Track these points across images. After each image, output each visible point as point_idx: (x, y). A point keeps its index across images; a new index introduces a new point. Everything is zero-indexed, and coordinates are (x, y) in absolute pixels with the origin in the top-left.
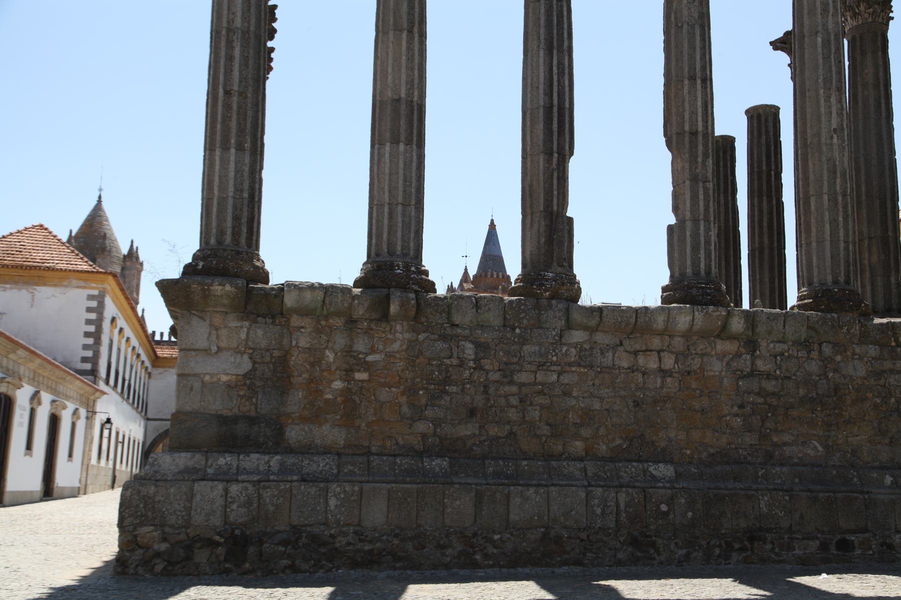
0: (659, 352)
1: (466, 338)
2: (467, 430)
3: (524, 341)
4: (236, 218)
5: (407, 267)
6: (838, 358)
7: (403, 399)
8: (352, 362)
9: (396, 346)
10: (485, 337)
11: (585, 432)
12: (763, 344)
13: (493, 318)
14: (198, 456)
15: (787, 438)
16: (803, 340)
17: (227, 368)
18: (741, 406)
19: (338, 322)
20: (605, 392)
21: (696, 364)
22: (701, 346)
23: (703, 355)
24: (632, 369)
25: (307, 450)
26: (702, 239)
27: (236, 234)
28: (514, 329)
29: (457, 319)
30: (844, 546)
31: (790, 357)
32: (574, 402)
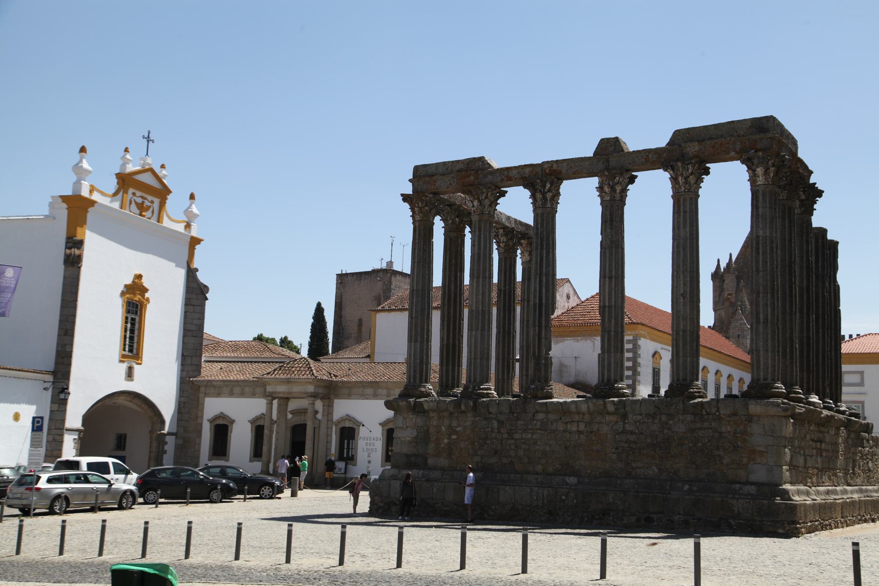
2: (493, 460)
3: (518, 419)
4: (415, 371)
5: (474, 387)
6: (671, 422)
7: (470, 447)
8: (452, 431)
9: (468, 423)
10: (501, 418)
12: (630, 416)
14: (397, 470)
17: (405, 435)
18: (617, 449)
19: (446, 414)
21: (595, 427)
23: (598, 423)
24: (565, 431)
25: (434, 468)
26: (606, 363)
27: (415, 378)
29: (491, 411)
31: (644, 422)
32: (537, 447)
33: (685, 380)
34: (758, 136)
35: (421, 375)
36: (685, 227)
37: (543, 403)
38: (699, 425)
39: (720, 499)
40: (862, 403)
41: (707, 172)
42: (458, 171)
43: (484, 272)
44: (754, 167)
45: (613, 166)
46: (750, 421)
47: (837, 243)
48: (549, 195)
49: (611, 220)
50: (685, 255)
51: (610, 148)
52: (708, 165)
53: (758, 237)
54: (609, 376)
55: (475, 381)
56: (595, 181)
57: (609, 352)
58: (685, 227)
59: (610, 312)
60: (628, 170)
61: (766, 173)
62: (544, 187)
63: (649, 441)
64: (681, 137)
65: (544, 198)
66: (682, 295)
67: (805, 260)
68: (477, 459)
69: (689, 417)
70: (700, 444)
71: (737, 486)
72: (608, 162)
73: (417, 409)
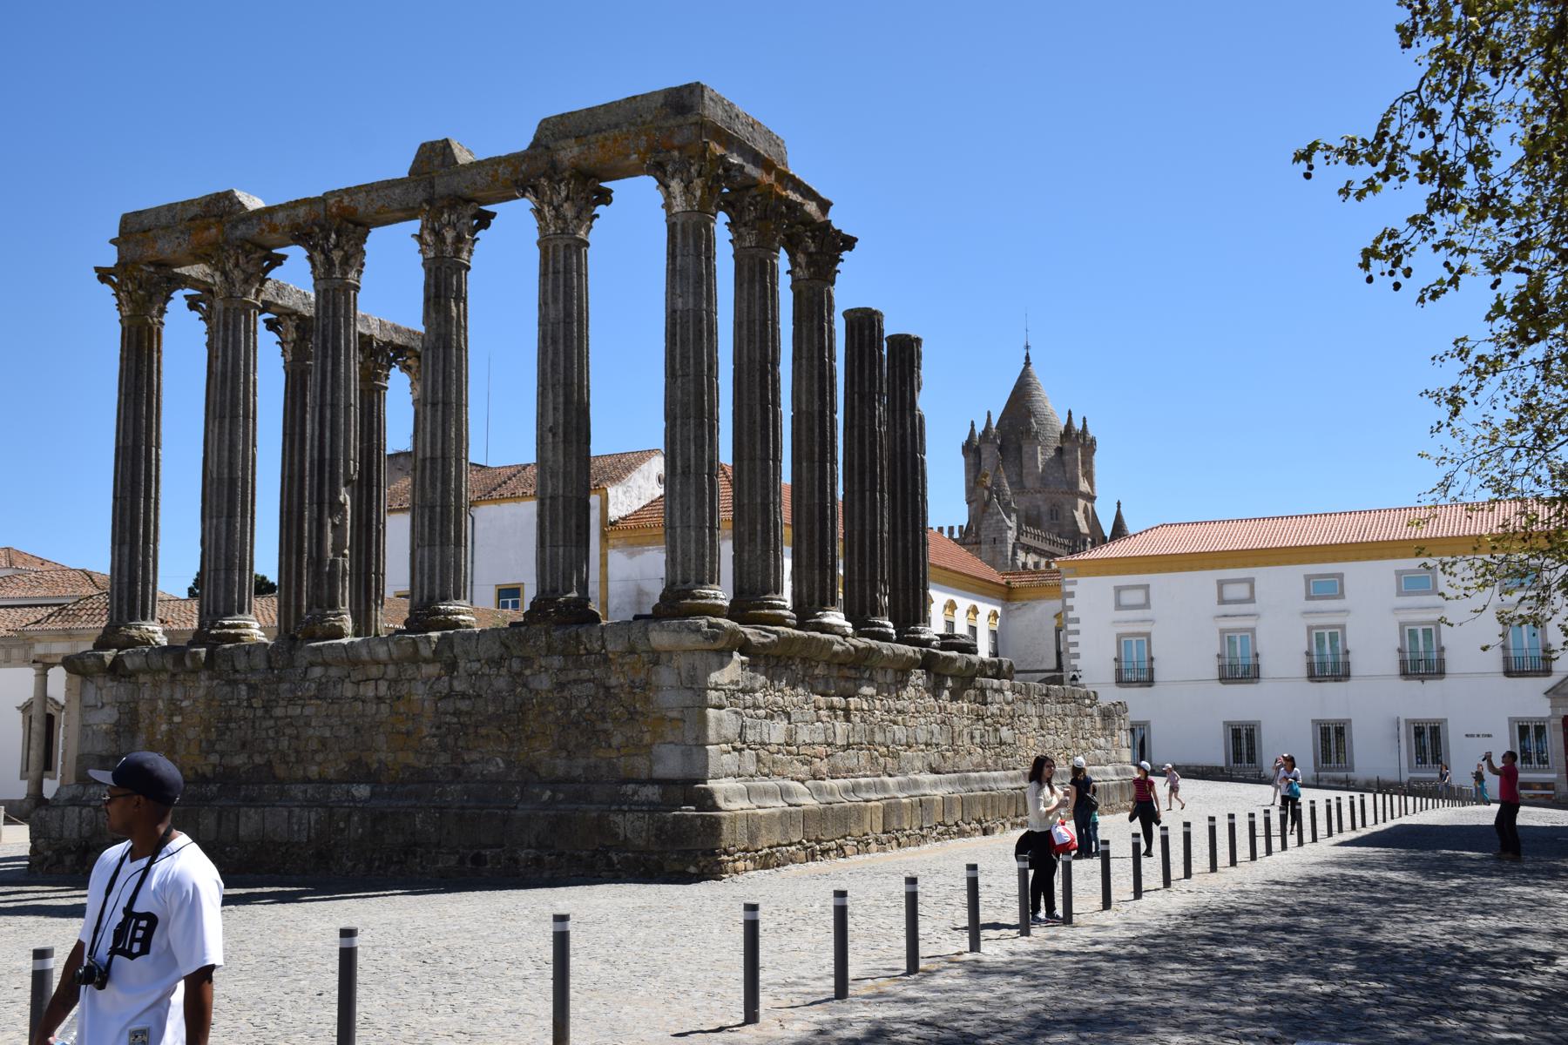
0: (376, 680)
1: (245, 681)
2: (239, 760)
3: (280, 680)
6: (528, 672)
8: (174, 707)
10: (254, 679)
11: (319, 757)
12: (462, 664)
13: (261, 663)
15: (475, 756)
16: (497, 656)
18: (439, 728)
20: (335, 721)
22: (410, 671)
23: (409, 681)
24: (355, 699)
27: (120, 612)
28: (272, 669)
30: (478, 860)
32: (311, 731)
33: (555, 591)
34: (672, 122)
35: (132, 607)
36: (555, 300)
37: (318, 648)
38: (572, 675)
39: (595, 814)
40: (1148, 635)
41: (605, 197)
42: (192, 219)
43: (234, 406)
44: (667, 180)
45: (446, 197)
46: (656, 663)
47: (918, 341)
48: (337, 255)
49: (437, 296)
50: (556, 353)
51: (435, 156)
52: (605, 185)
53: (674, 311)
54: (432, 590)
55: (216, 612)
56: (415, 226)
57: (431, 545)
58: (555, 300)
59: (433, 469)
60: (468, 201)
61: (687, 189)
62: (327, 238)
63: (491, 709)
64: (553, 130)
65: (329, 262)
66: (551, 430)
67: (816, 362)
68: (214, 758)
69: (557, 662)
70: (574, 712)
71: (630, 788)
72: (432, 187)
73: (116, 670)
